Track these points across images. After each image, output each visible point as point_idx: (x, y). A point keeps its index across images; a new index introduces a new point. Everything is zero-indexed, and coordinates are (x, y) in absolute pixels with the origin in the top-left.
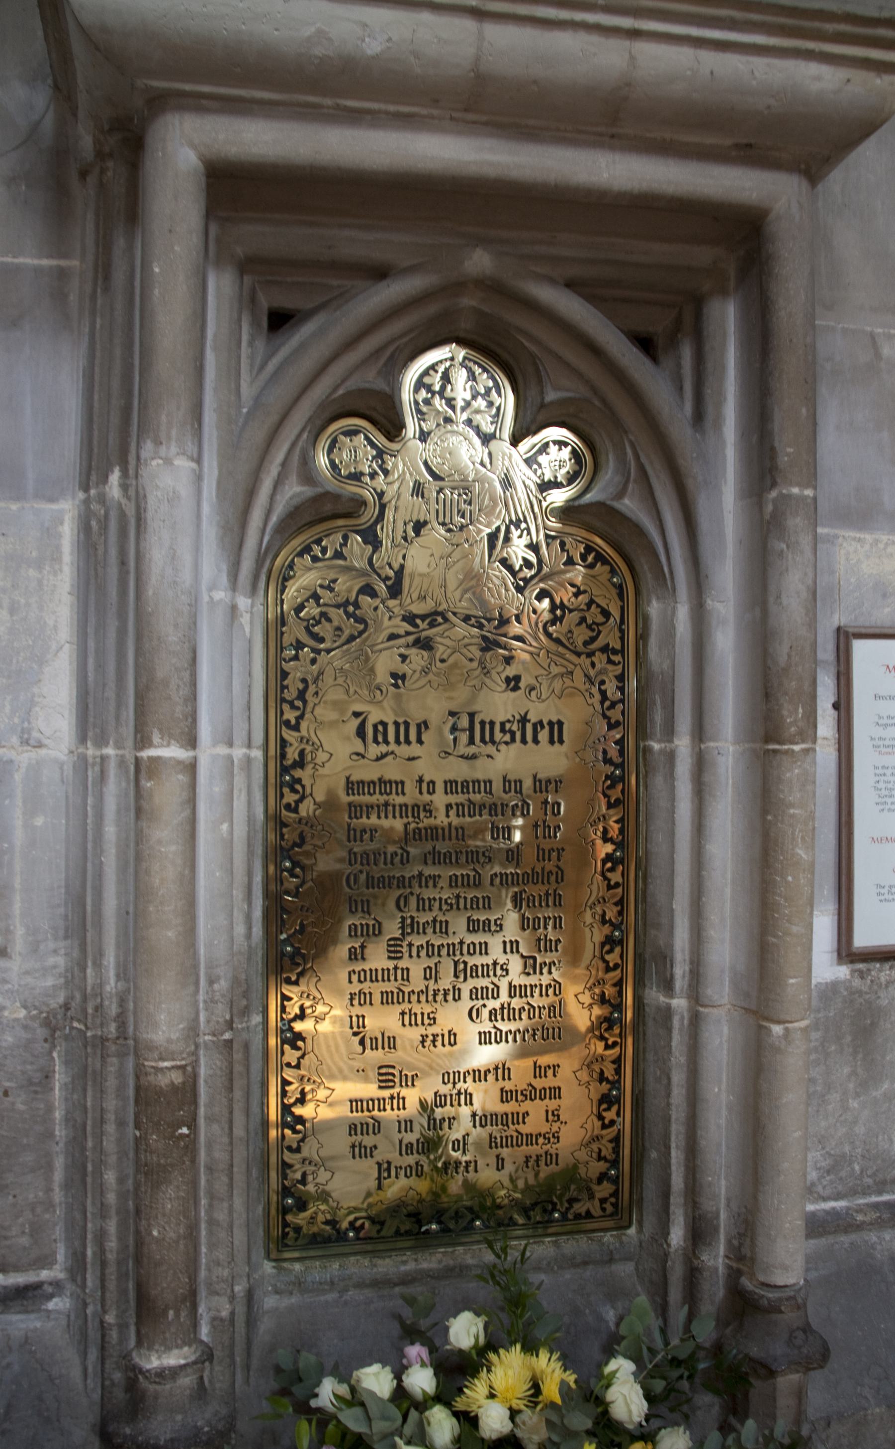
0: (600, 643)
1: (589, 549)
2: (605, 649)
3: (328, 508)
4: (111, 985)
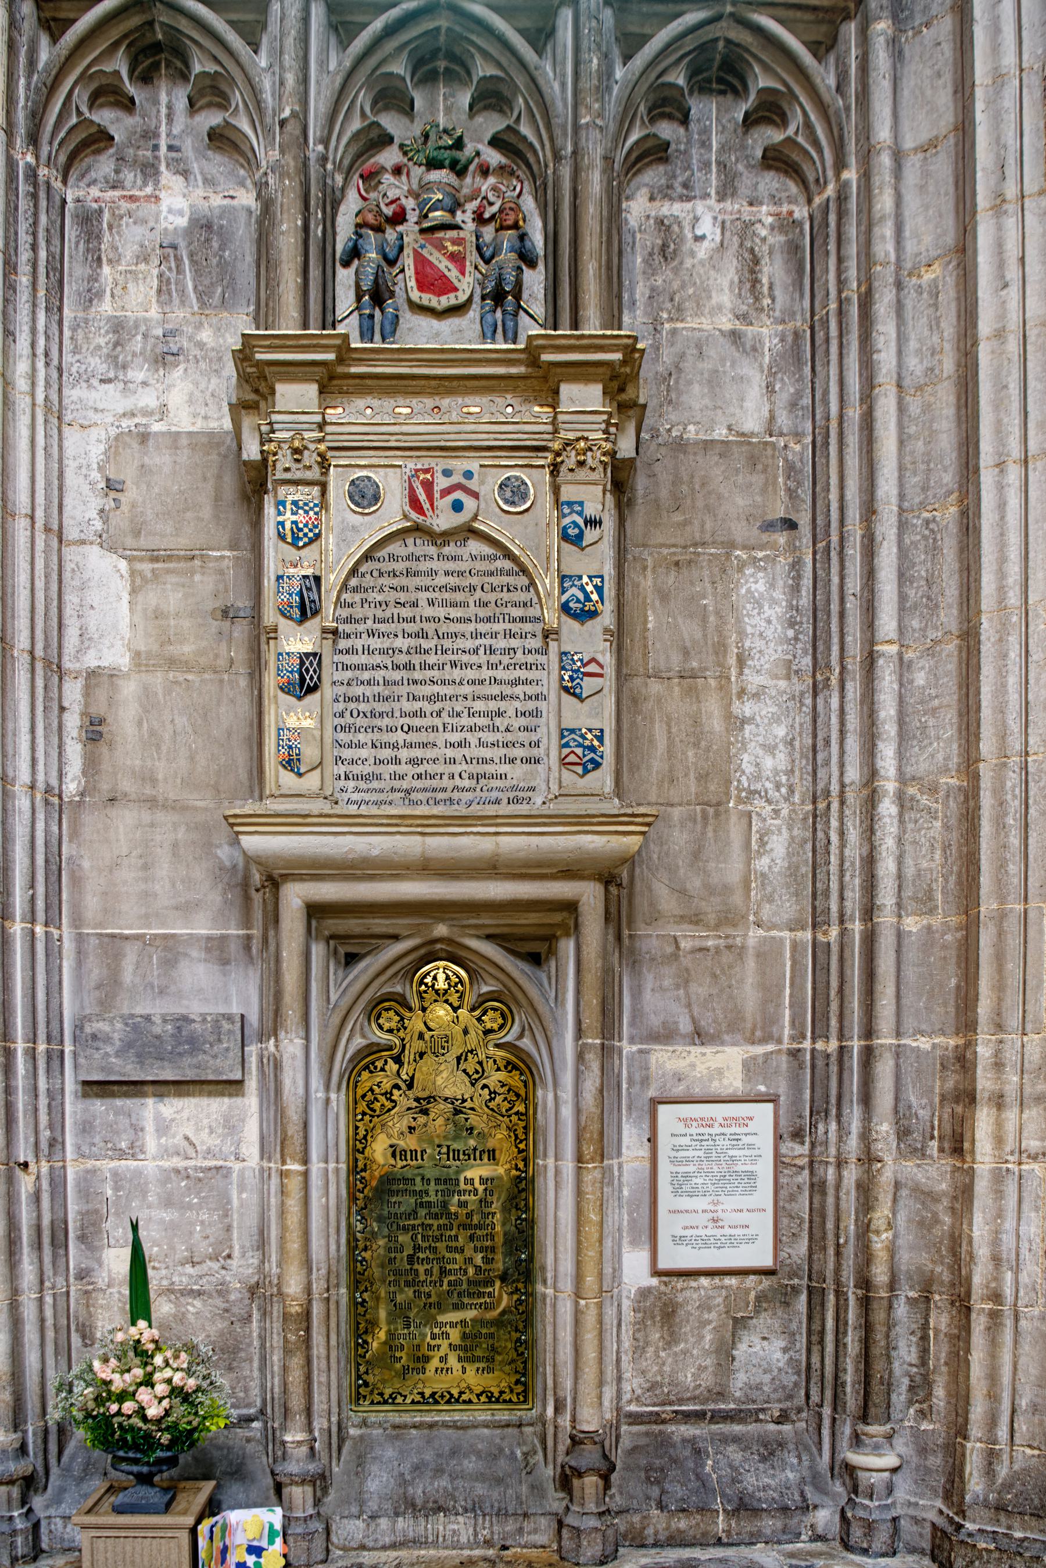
0: (515, 1110)
1: (508, 1063)
2: (517, 1113)
3: (375, 1049)
4: (275, 1270)
